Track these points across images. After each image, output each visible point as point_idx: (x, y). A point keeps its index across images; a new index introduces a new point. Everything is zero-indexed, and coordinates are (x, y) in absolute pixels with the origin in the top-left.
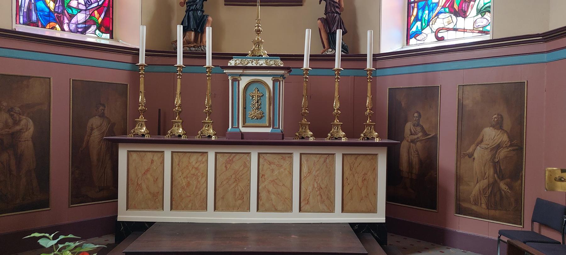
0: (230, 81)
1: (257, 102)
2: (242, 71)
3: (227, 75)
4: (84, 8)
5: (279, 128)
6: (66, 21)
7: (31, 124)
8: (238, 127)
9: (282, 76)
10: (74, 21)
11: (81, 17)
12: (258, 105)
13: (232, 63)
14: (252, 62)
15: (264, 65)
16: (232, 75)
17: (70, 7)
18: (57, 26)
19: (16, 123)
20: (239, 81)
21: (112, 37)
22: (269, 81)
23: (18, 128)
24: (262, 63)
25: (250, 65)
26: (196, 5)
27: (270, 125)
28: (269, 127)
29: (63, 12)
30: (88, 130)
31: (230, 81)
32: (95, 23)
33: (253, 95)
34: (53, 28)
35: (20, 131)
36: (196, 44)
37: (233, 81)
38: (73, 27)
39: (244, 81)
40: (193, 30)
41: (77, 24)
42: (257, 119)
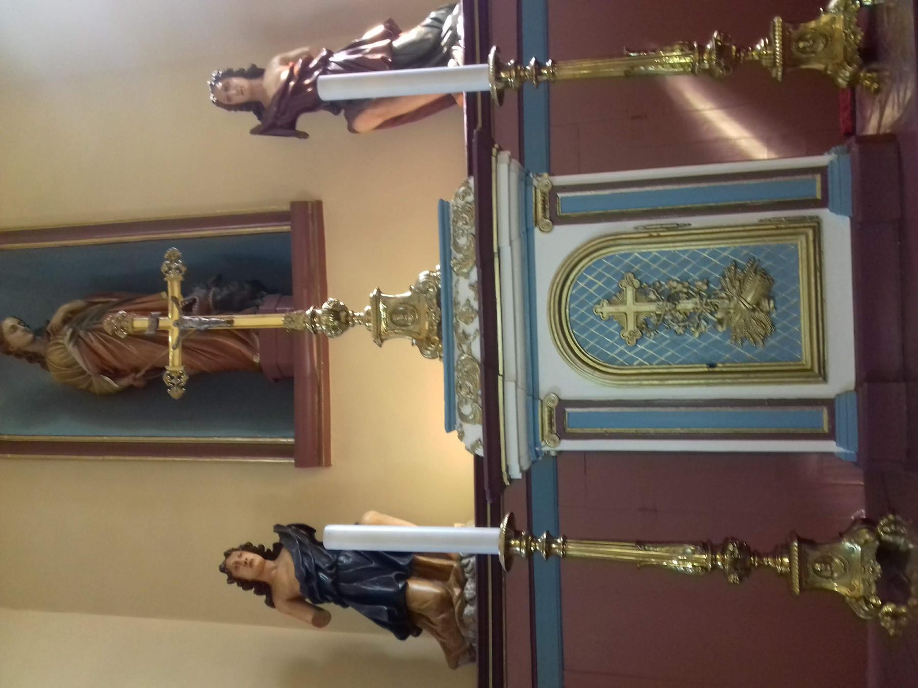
0: (568, 445)
1: (673, 298)
2: (511, 386)
5: (822, 170)
8: (828, 403)
12: (689, 297)
14: (466, 336)
15: (474, 276)
20: (563, 404)
25: (476, 348)
26: (318, 568)
27: (802, 219)
28: (817, 228)
31: (568, 445)
33: (631, 326)
36: (452, 579)
37: (563, 434)
40: (400, 585)
42: (769, 297)
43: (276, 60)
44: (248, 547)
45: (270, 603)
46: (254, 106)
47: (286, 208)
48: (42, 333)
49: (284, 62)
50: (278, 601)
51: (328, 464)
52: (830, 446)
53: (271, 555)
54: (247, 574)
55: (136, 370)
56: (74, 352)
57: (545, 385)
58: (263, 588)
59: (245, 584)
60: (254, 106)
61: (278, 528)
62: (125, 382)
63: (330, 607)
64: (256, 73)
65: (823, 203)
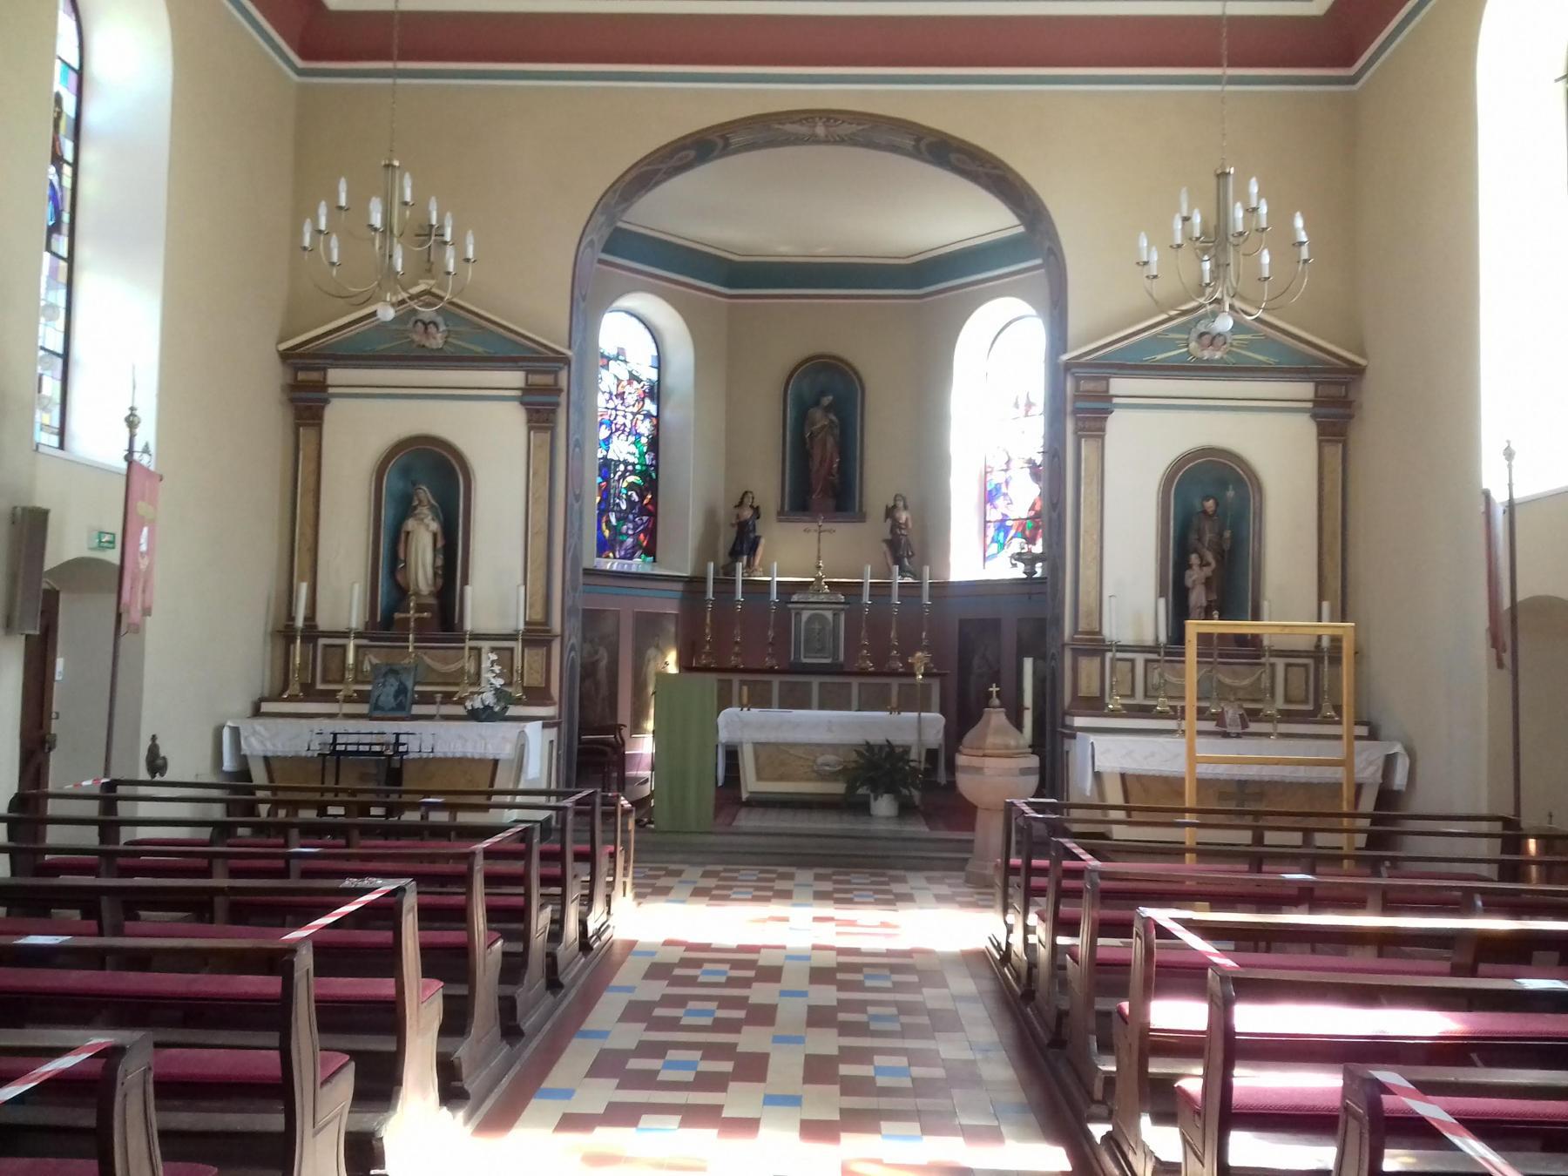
3: (790, 609)
4: (630, 532)
6: (618, 548)
7: (606, 655)
9: (843, 609)
10: (624, 547)
11: (630, 541)
13: (795, 598)
15: (825, 600)
16: (795, 609)
17: (621, 534)
18: (611, 555)
19: (596, 652)
21: (654, 561)
22: (829, 615)
23: (597, 657)
24: (822, 598)
29: (615, 540)
30: (646, 659)
32: (641, 547)
34: (608, 557)
35: (597, 661)
38: (623, 553)
39: (805, 615)
41: (626, 550)
43: (909, 516)
44: (753, 498)
45: (736, 507)
46: (895, 507)
47: (864, 510)
48: (828, 409)
49: (907, 519)
50: (737, 511)
51: (780, 521)
52: (792, 658)
53: (751, 506)
54: (746, 500)
55: (812, 448)
56: (819, 426)
57: (805, 612)
58: (741, 504)
59: (742, 499)
60: (895, 507)
61: (758, 507)
62: (808, 440)
63: (736, 529)
64: (906, 507)
65: (833, 659)
